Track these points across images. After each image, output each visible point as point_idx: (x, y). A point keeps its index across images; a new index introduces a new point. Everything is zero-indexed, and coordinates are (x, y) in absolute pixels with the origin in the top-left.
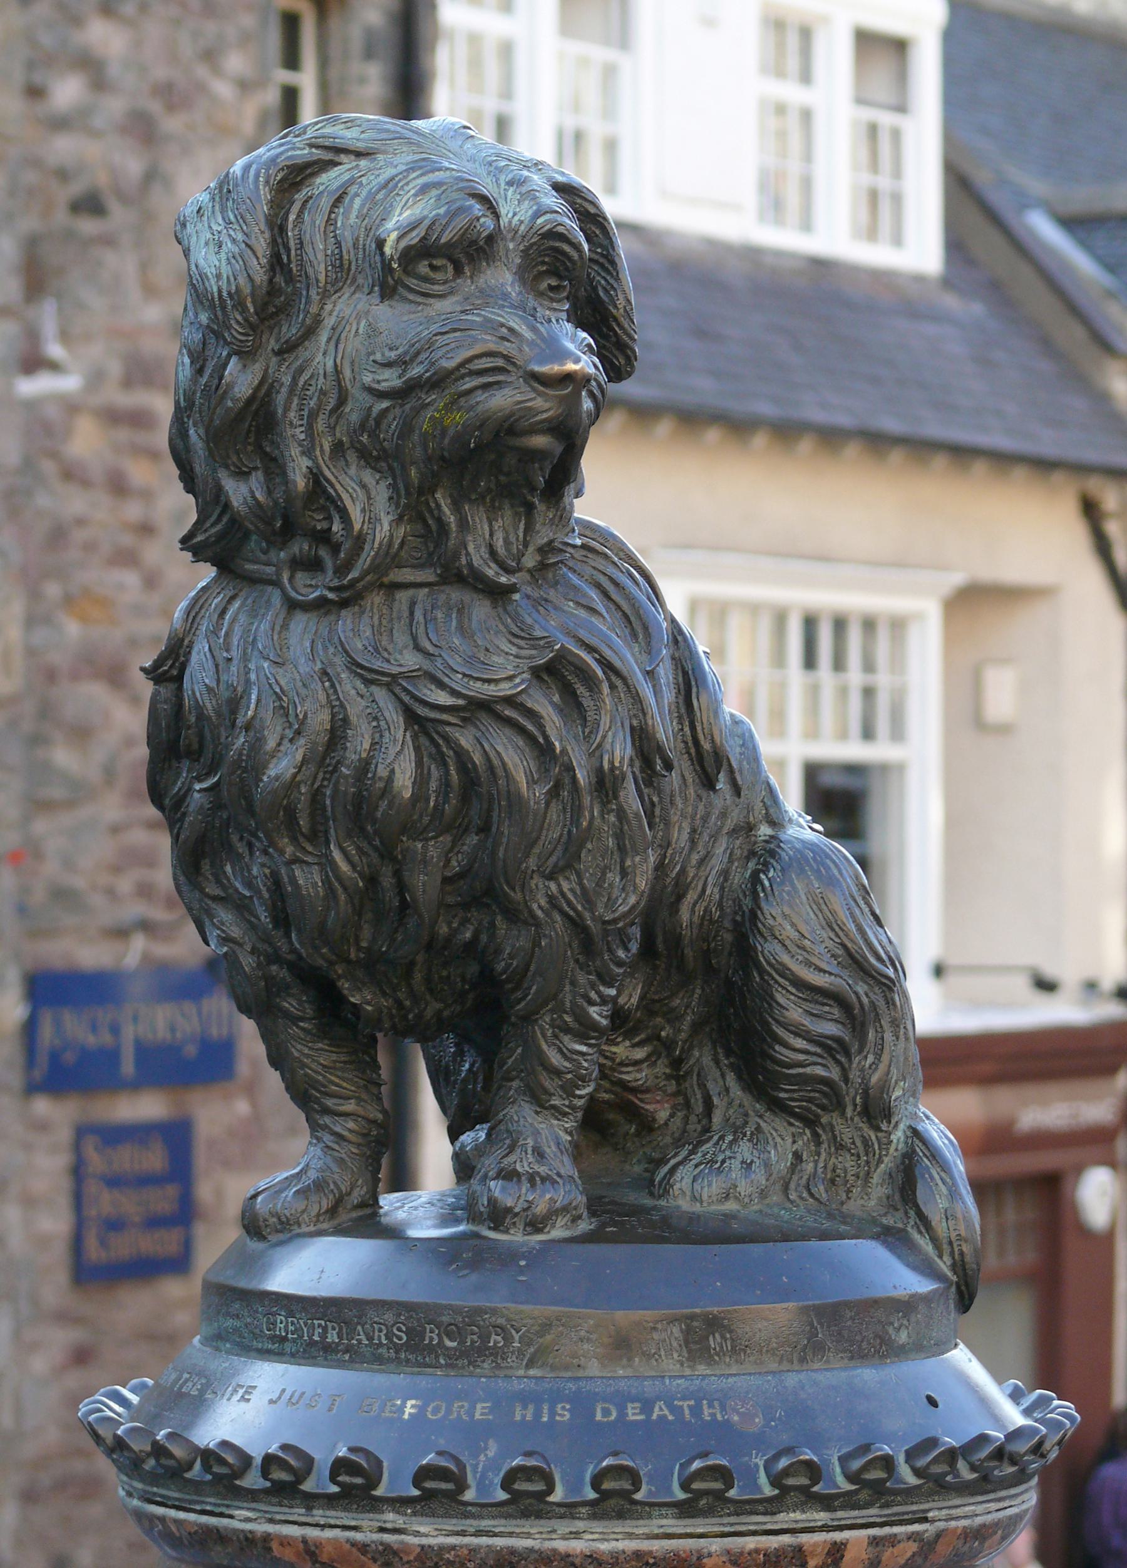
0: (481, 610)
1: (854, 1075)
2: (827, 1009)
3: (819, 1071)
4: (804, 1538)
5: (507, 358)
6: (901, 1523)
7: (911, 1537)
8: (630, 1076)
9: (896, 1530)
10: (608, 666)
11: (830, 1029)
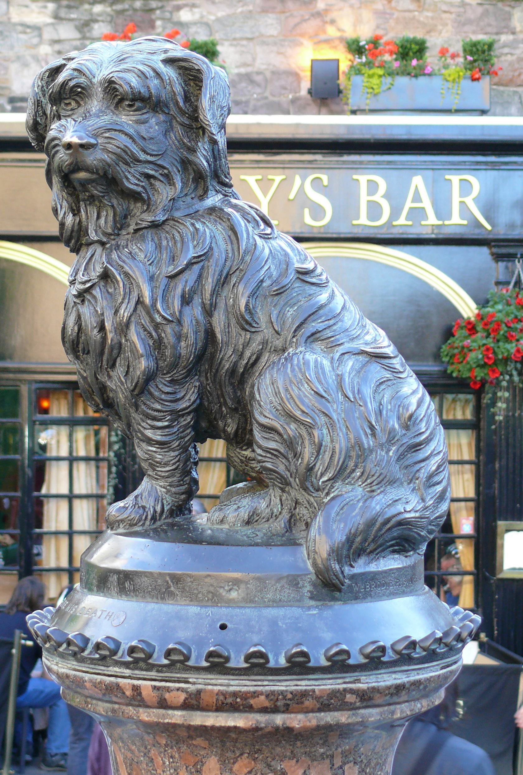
2: (272, 435)
4: (119, 680)
5: (59, 139)
6: (174, 682)
7: (178, 689)
9: (168, 684)
11: (272, 445)
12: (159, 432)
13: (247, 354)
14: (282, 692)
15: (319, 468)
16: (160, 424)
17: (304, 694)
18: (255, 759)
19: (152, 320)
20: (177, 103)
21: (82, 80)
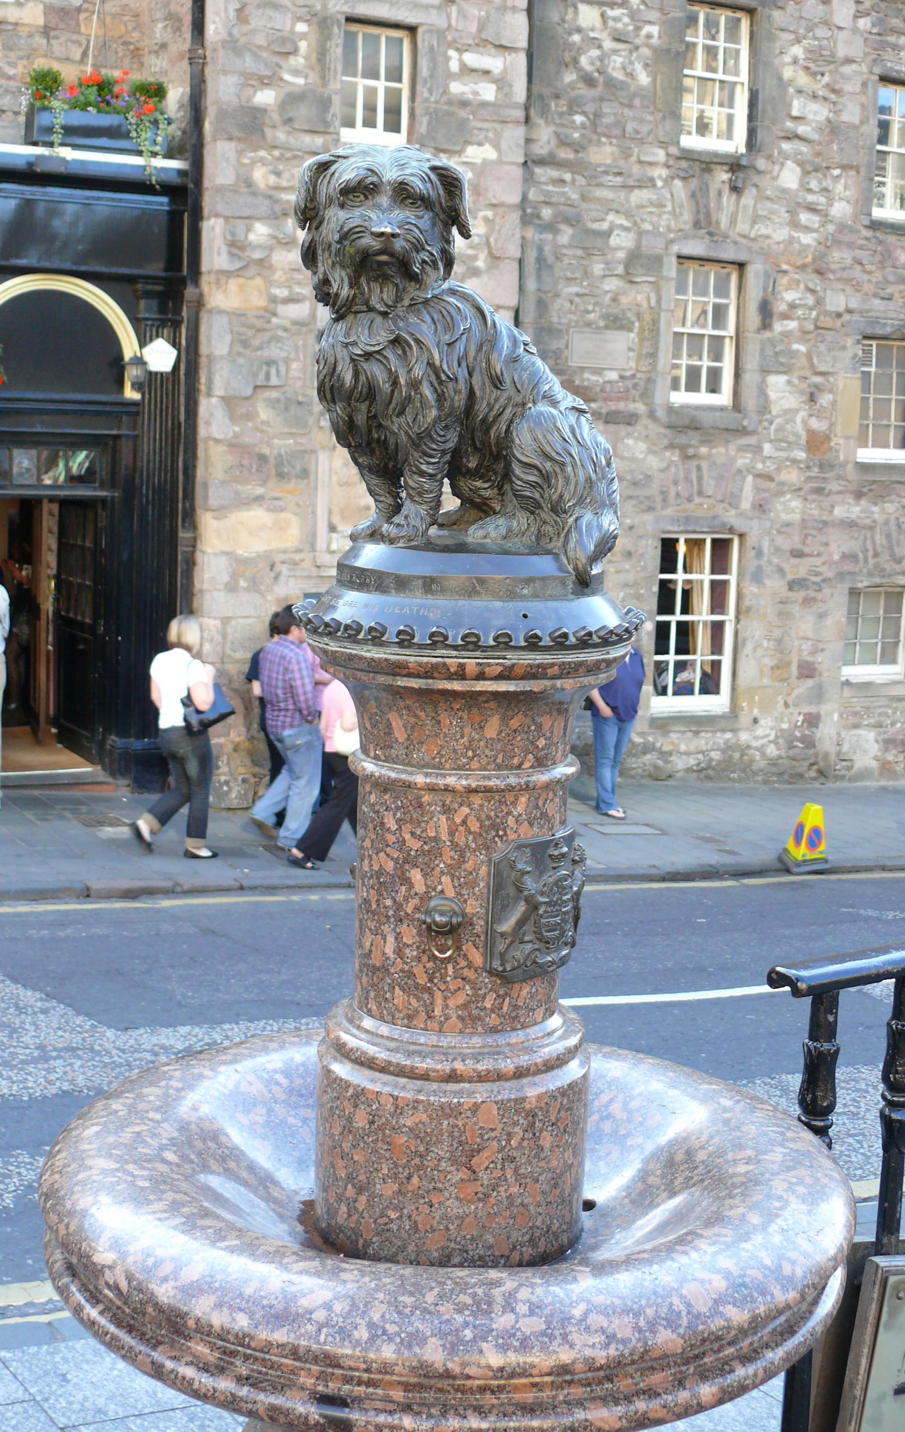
0: (379, 319)
1: (546, 496)
3: (528, 494)
4: (447, 660)
8: (483, 493)
10: (418, 341)
11: (532, 478)
12: (431, 467)
13: (497, 407)
14: (569, 663)
15: (567, 496)
16: (433, 460)
17: (581, 664)
18: (526, 716)
19: (438, 377)
20: (441, 203)
21: (375, 179)
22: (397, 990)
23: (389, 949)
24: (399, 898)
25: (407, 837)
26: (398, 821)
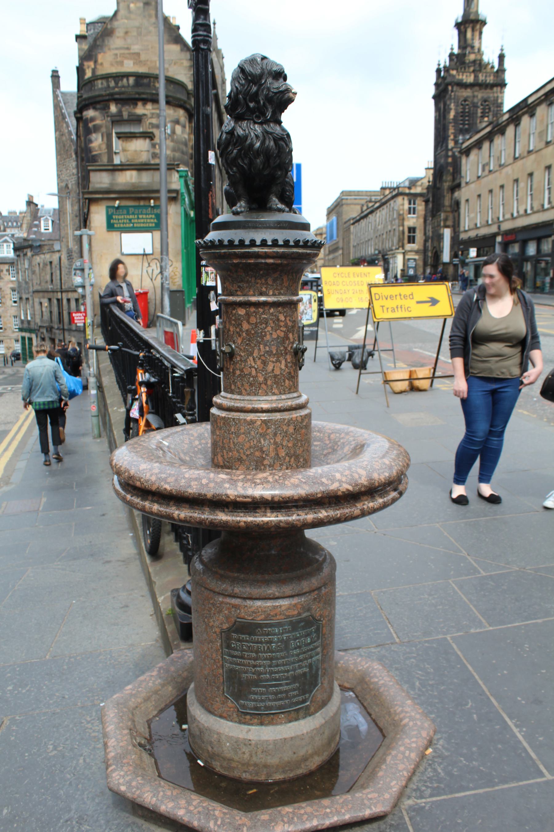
22: (287, 381)
23: (283, 367)
24: (286, 345)
25: (288, 322)
26: (285, 317)
